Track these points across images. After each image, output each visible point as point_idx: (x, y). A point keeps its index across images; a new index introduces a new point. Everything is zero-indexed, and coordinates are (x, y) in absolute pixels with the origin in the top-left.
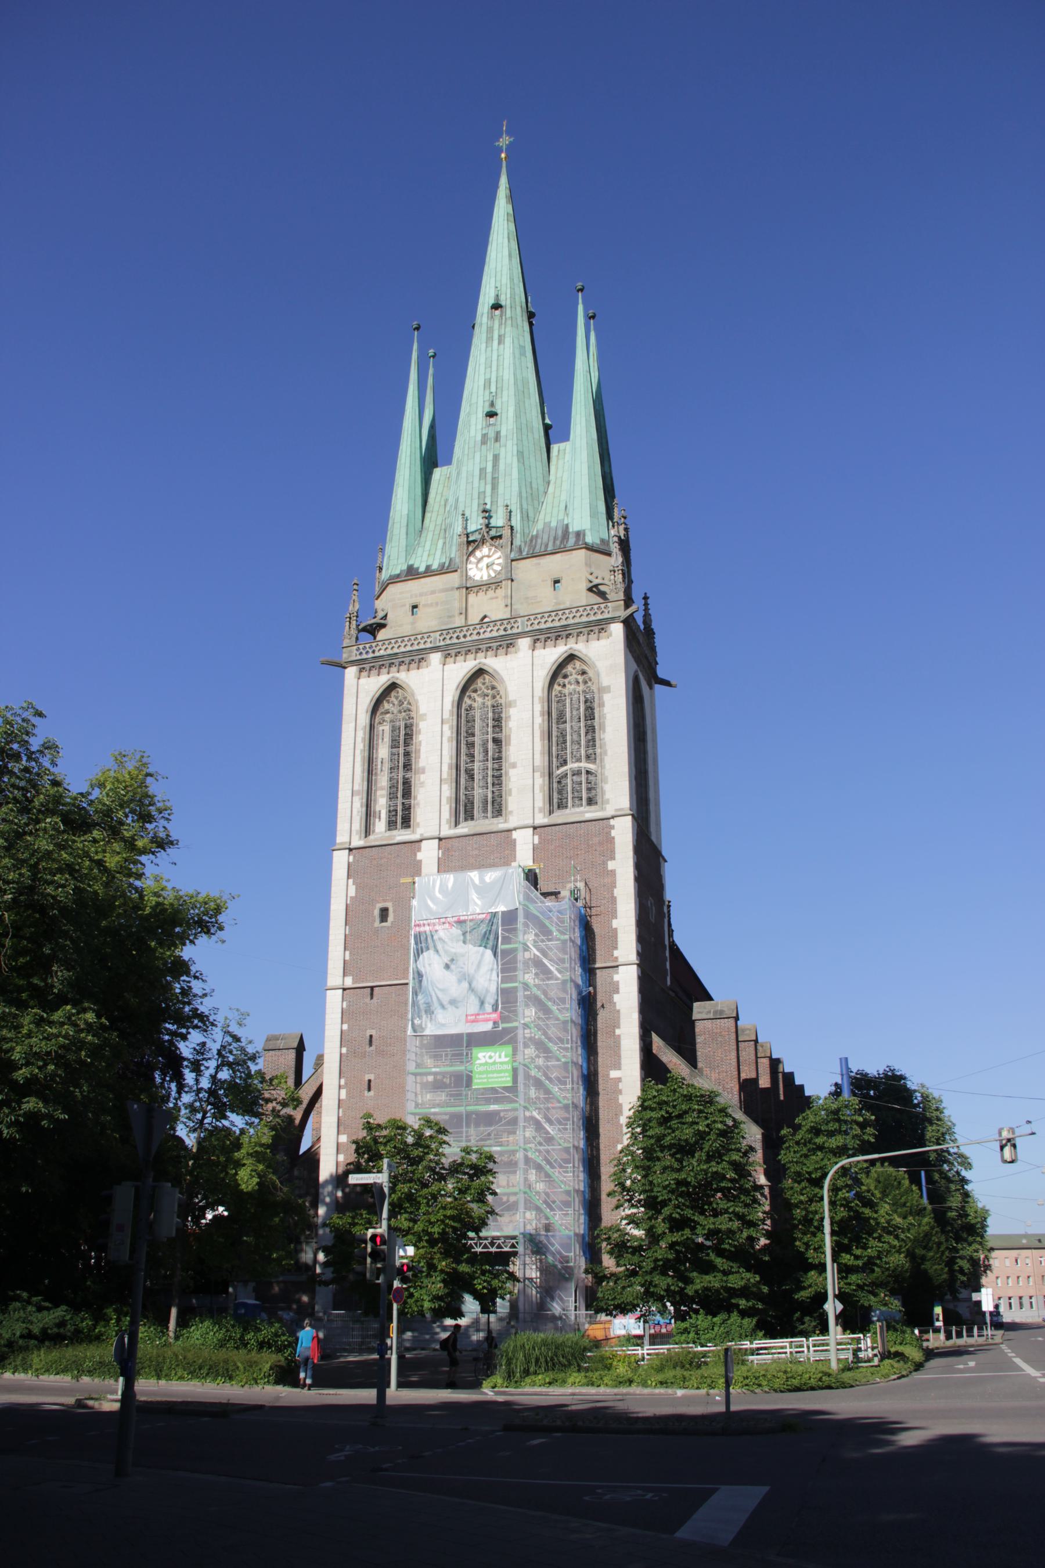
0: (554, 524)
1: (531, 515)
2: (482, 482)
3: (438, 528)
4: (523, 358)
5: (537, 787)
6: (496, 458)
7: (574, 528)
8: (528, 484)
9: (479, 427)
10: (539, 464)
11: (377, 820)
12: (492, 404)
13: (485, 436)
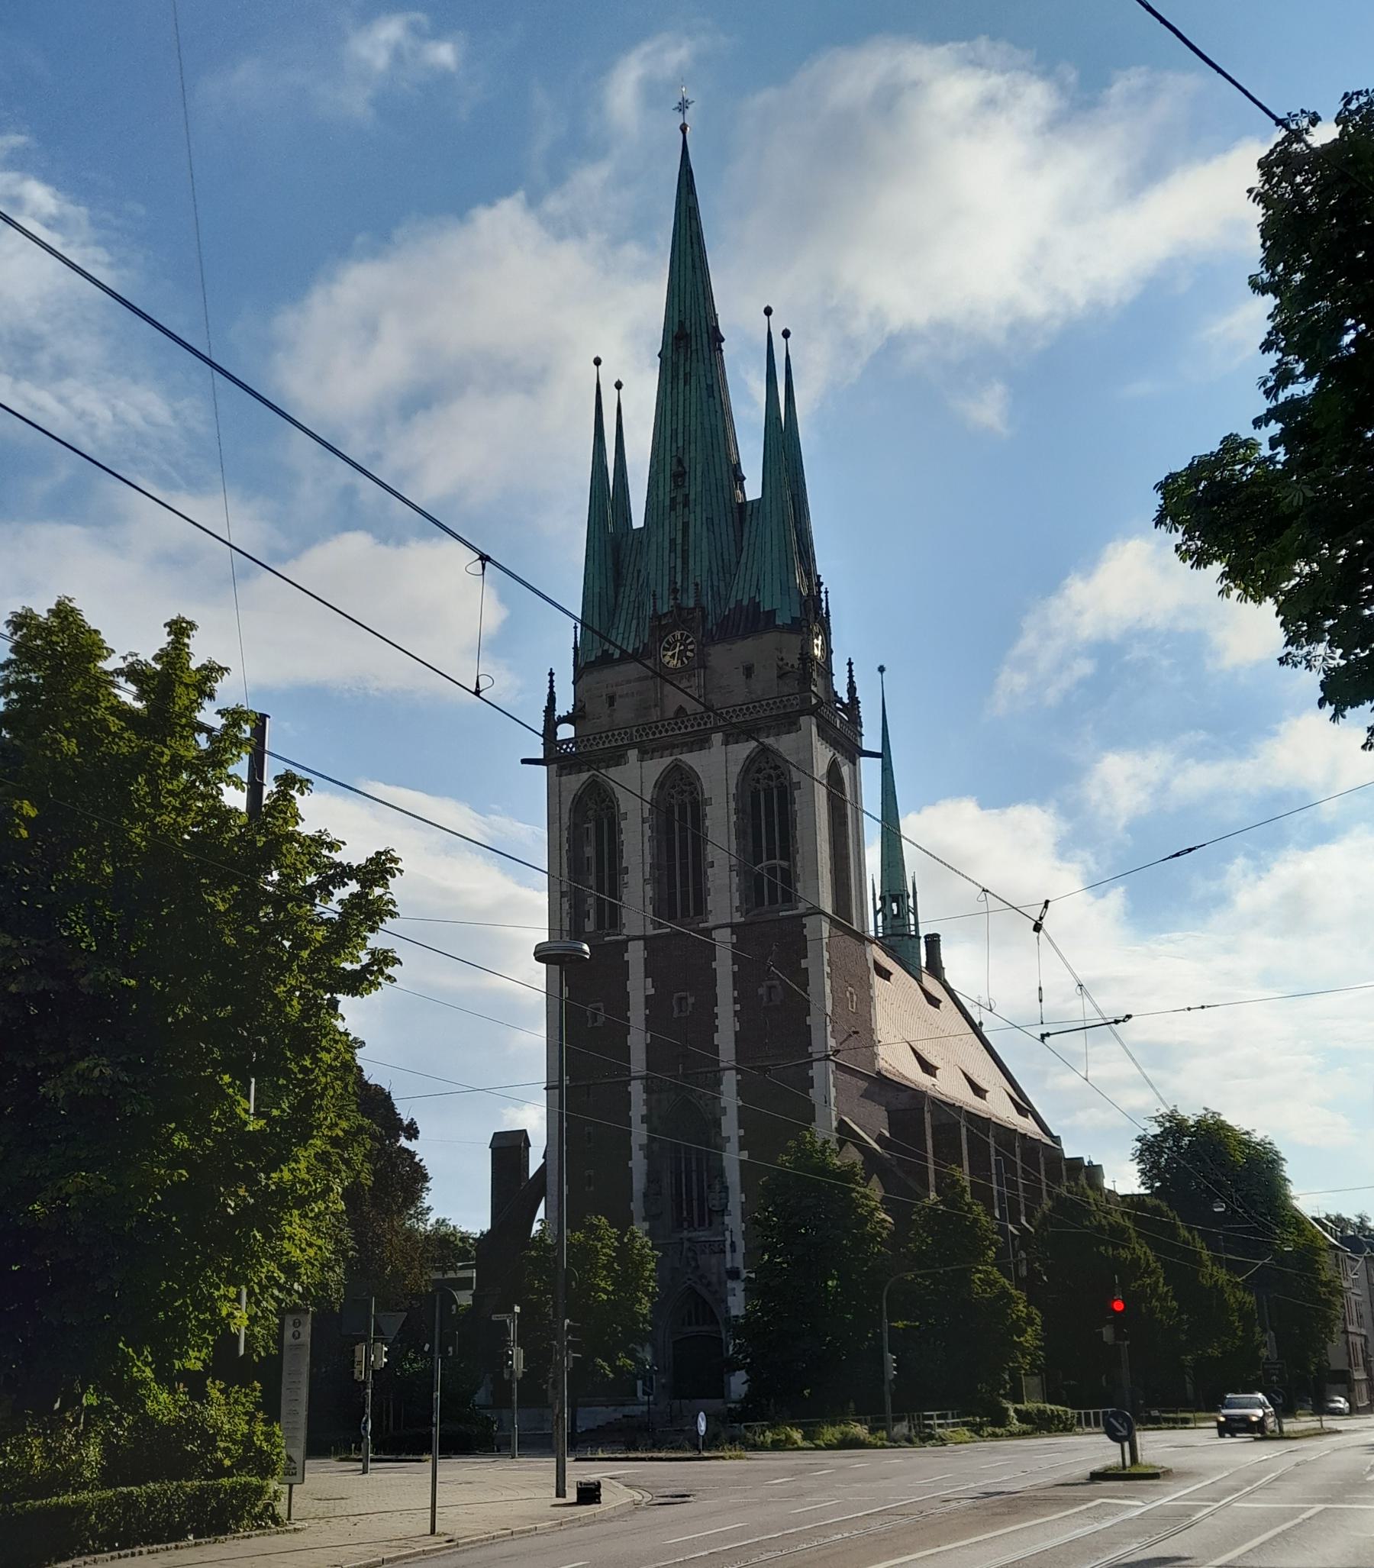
0: (745, 602)
1: (723, 591)
2: (673, 555)
3: (632, 605)
4: (711, 399)
5: (734, 886)
6: (686, 525)
7: (766, 607)
8: (719, 556)
9: (668, 489)
10: (731, 530)
11: (586, 920)
12: (680, 462)
13: (673, 500)
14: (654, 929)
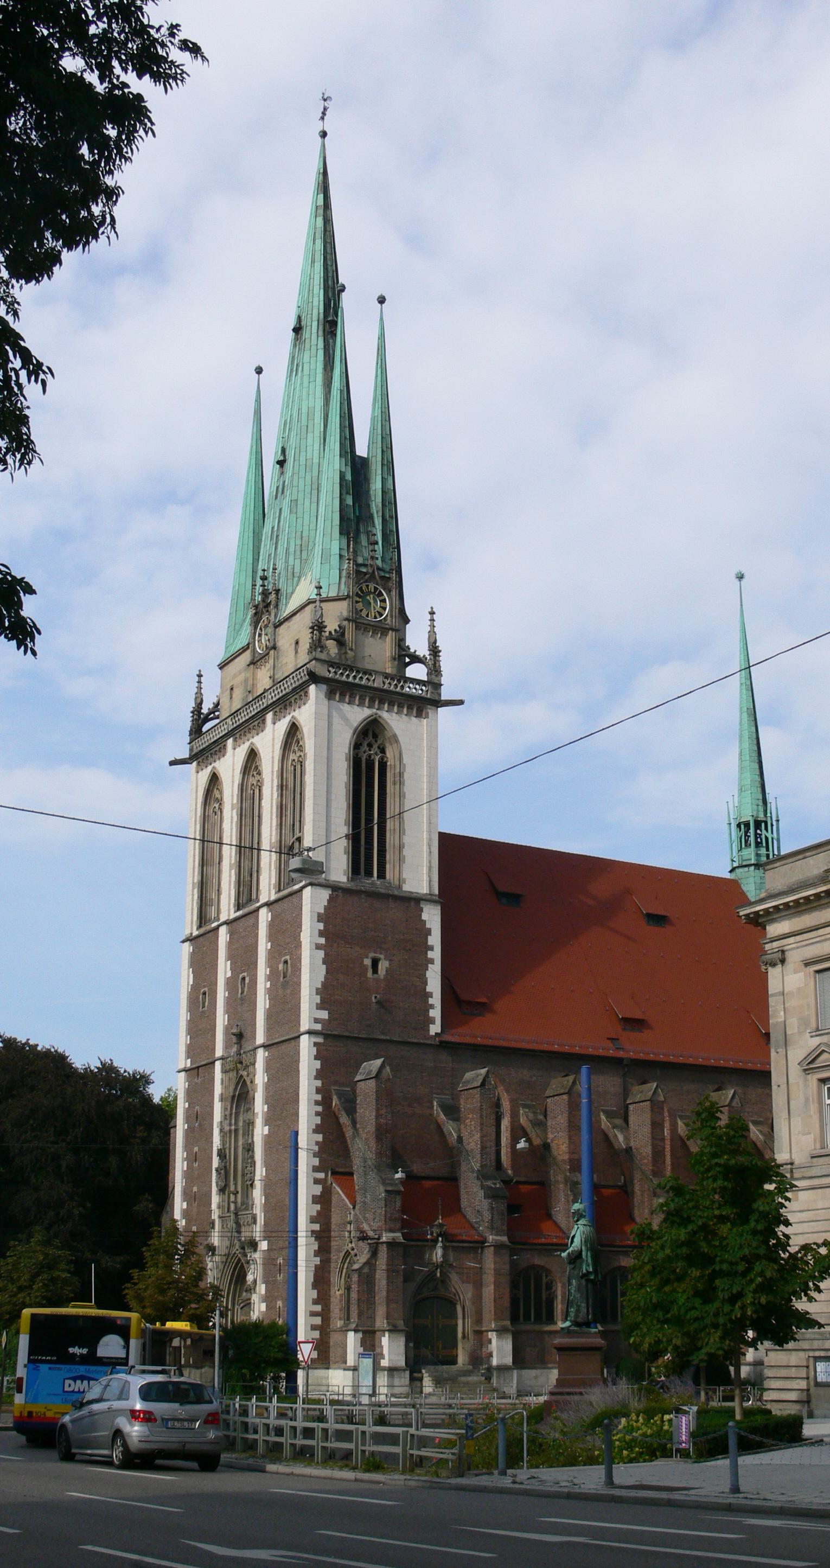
1: (297, 570)
8: (299, 534)
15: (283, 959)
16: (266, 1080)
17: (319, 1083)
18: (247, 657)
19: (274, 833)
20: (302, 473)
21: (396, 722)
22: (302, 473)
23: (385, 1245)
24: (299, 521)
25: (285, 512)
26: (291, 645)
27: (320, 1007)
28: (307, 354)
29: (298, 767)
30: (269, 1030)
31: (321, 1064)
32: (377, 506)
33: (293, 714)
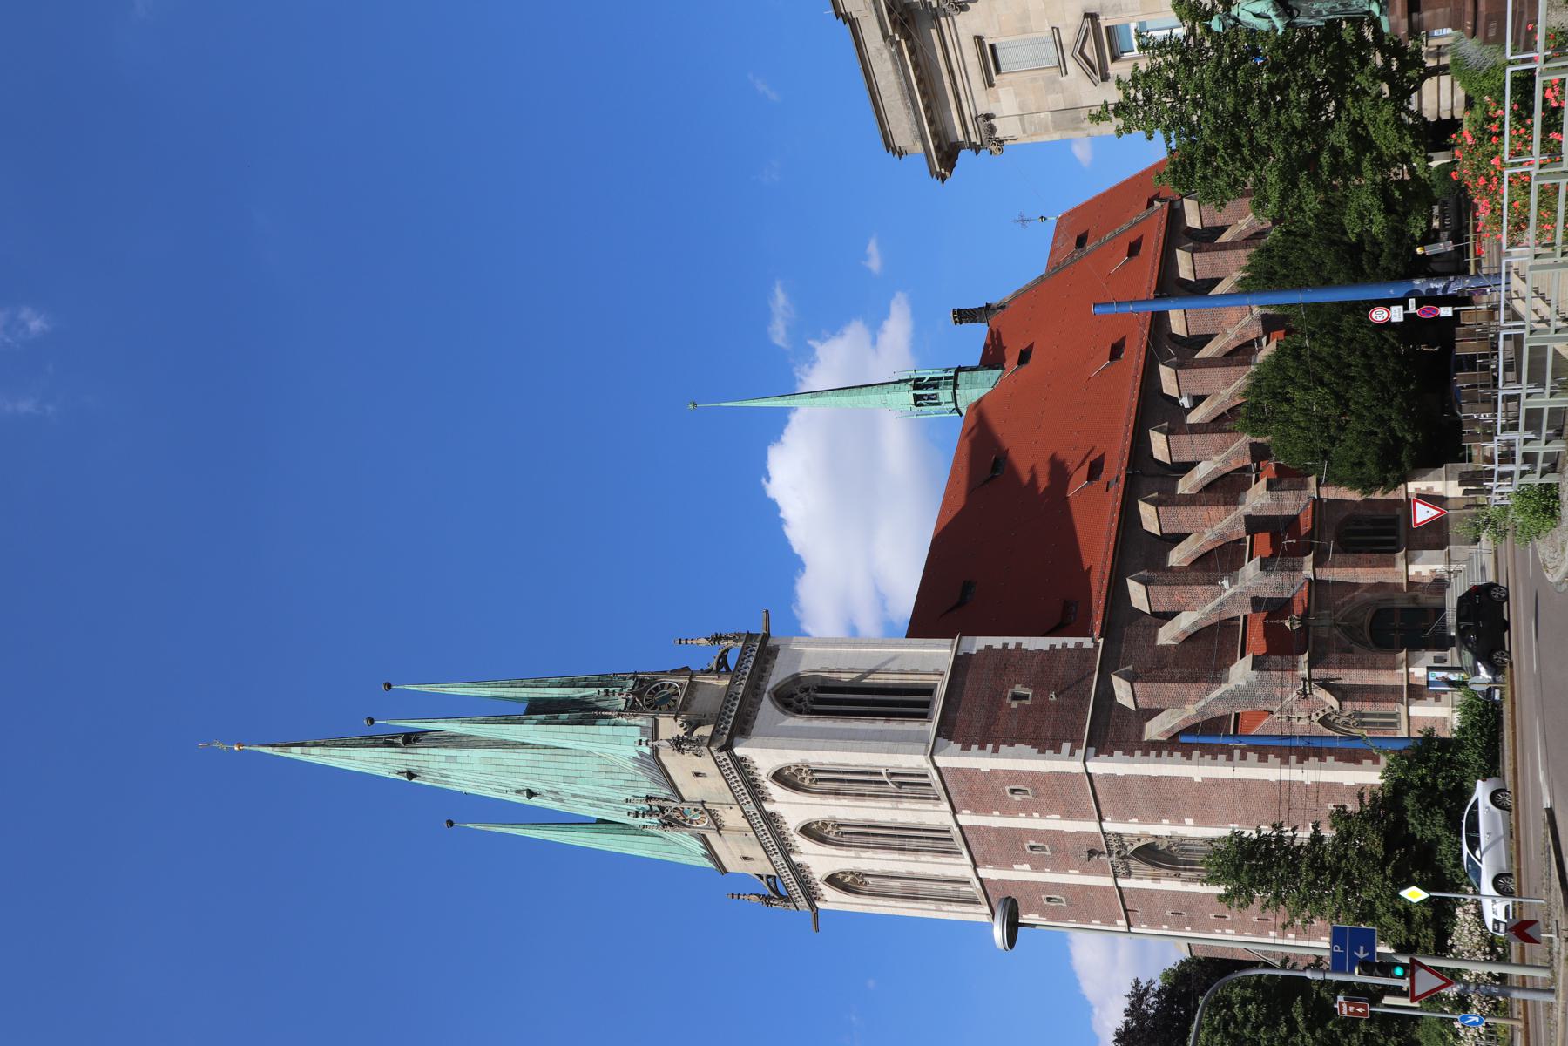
6: (574, 796)
8: (596, 775)
14: (963, 858)
15: (1009, 795)
16: (1136, 820)
17: (1138, 753)
18: (713, 837)
19: (882, 805)
20: (540, 771)
21: (778, 674)
22: (540, 771)
23: (1312, 671)
24: (583, 774)
25: (575, 789)
26: (699, 783)
27: (1058, 750)
28: (431, 765)
29: (818, 775)
30: (1083, 816)
31: (1119, 750)
32: (574, 693)
33: (763, 778)
